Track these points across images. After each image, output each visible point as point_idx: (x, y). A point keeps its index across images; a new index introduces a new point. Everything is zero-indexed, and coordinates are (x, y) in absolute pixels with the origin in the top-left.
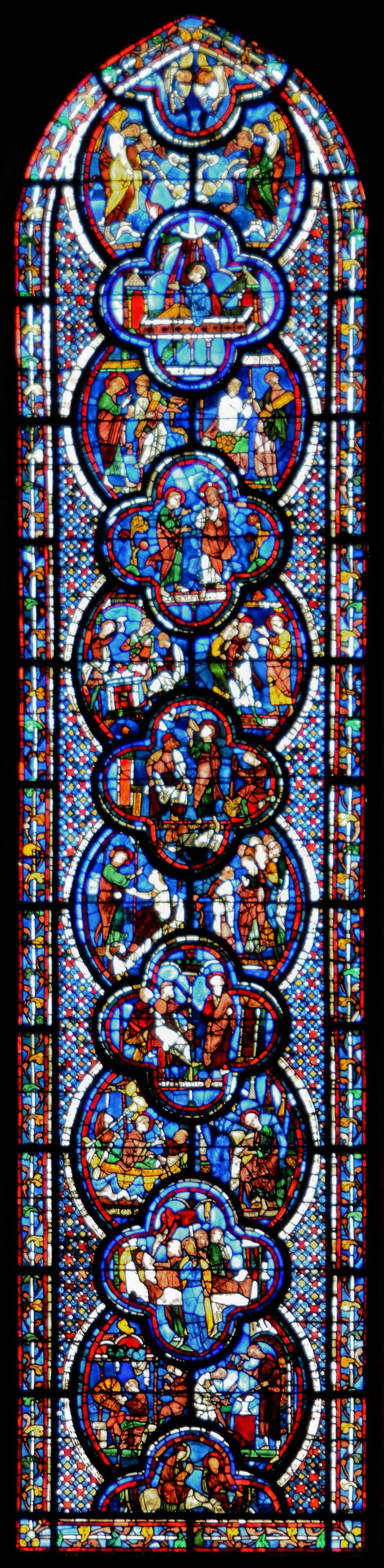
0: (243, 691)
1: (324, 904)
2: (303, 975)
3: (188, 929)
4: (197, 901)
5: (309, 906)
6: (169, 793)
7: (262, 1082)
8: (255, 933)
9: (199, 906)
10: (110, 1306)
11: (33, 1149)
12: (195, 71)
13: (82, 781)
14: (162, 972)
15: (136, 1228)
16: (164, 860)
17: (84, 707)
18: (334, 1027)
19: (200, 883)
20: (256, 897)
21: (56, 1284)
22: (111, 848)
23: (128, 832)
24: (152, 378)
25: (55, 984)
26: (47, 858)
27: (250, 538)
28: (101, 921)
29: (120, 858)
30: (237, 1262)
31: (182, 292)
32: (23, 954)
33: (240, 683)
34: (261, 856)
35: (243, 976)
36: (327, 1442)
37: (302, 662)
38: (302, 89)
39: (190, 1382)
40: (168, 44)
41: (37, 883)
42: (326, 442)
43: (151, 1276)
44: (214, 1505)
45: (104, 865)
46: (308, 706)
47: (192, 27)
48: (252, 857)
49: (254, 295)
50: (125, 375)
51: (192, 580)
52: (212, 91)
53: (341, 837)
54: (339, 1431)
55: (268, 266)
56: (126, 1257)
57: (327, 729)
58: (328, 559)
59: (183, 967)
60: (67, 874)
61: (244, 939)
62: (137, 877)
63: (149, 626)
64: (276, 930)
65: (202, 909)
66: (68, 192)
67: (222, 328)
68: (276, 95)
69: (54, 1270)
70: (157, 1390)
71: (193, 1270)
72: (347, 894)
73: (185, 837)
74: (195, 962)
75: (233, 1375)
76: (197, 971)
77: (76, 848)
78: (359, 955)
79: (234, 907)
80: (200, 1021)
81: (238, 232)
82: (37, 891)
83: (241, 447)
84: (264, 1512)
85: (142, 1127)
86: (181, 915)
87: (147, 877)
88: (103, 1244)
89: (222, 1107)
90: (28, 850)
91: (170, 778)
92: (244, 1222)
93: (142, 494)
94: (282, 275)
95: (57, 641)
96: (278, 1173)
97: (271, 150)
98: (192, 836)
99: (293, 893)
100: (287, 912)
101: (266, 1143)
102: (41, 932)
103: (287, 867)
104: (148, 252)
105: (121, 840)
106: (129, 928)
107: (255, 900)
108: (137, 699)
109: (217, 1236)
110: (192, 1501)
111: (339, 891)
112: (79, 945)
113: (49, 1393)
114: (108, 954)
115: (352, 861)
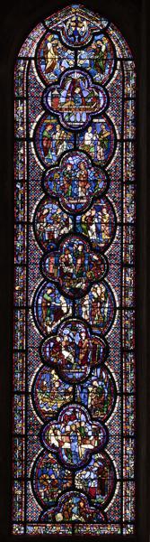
0: (93, 234)
1: (121, 308)
3: (73, 316)
5: (115, 309)
6: (66, 269)
7: (99, 370)
8: (97, 318)
10: (45, 449)
11: (18, 393)
12: (76, 21)
13: (36, 264)
15: (55, 421)
17: (37, 239)
18: (124, 351)
21: (26, 441)
23: (52, 282)
24: (61, 126)
25: (26, 335)
27: (95, 181)
29: (50, 291)
30: (90, 433)
31: (72, 97)
33: (91, 231)
34: (99, 291)
35: (92, 333)
36: (122, 496)
37: (113, 225)
38: (113, 30)
39: (74, 475)
40: (67, 13)
42: (121, 149)
43: (59, 438)
44: (82, 519)
46: (115, 240)
47: (75, 8)
49: (98, 98)
50: (52, 124)
51: (75, 196)
52: (84, 28)
54: (126, 492)
55: (102, 89)
56: (51, 431)
57: (122, 248)
58: (122, 190)
59: (72, 330)
61: (93, 320)
63: (60, 211)
64: (104, 317)
66: (33, 62)
67: (86, 109)
68: (104, 32)
69: (26, 436)
70: (61, 478)
71: (75, 436)
75: (88, 473)
80: (77, 349)
81: (91, 77)
83: (92, 150)
84: (100, 522)
85: (57, 386)
86: (71, 312)
88: (43, 427)
89: (86, 378)
90: (17, 288)
91: (67, 264)
92: (92, 419)
93: (58, 165)
94: (107, 92)
95: (28, 216)
96: (104, 403)
97: (103, 50)
101: (100, 392)
104: (60, 83)
106: (52, 316)
108: (56, 236)
109: (83, 424)
110: (74, 518)
113: (23, 479)
115: (131, 294)
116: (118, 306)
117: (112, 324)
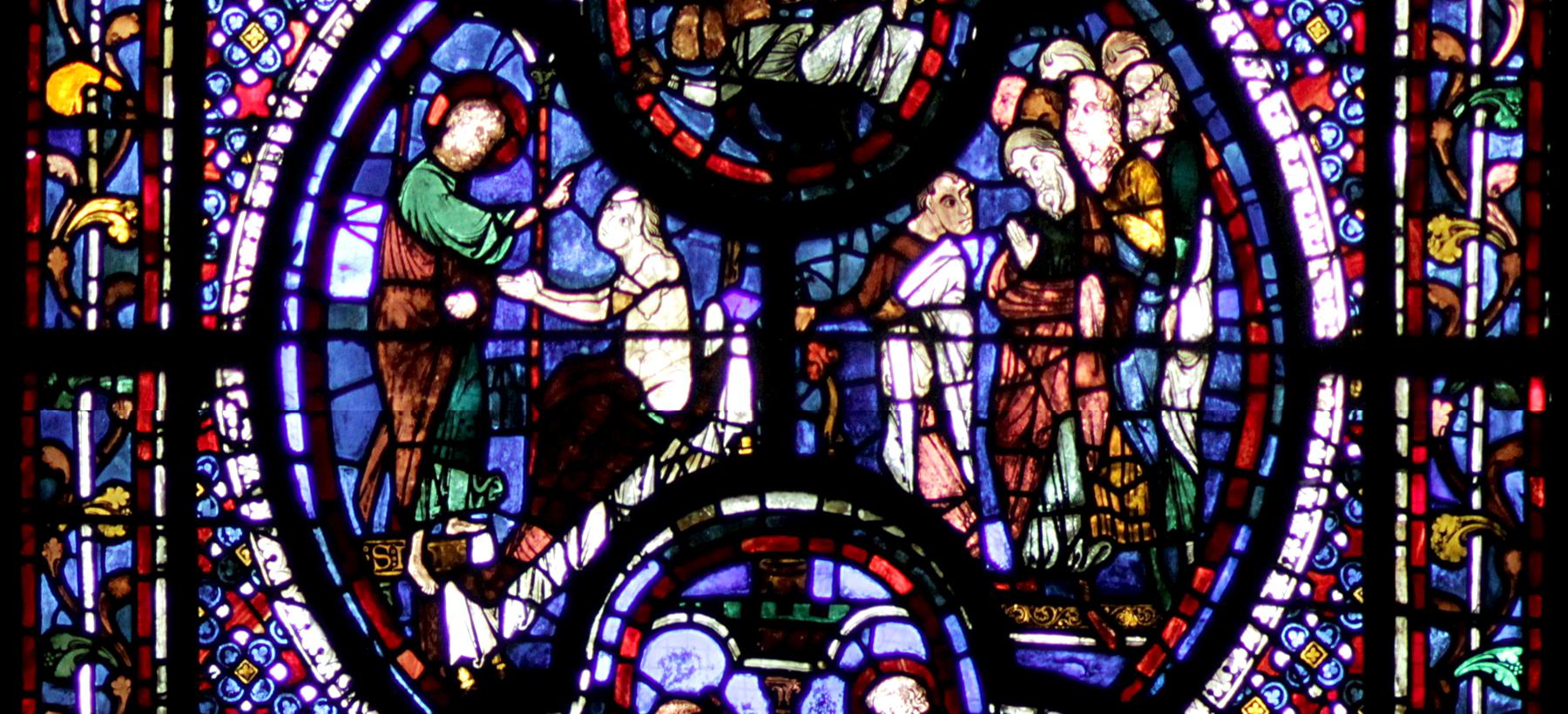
1: (1368, 354)
2: (1276, 675)
4: (812, 332)
5: (1308, 359)
8: (1067, 482)
9: (818, 355)
14: (654, 661)
16: (665, 141)
19: (825, 248)
20: (1074, 318)
22: (430, 83)
26: (151, 124)
28: (386, 417)
32: (42, 566)
34: (1092, 132)
41: (107, 241)
45: (400, 165)
48: (1054, 132)
53: (1446, 47)
59: (748, 637)
60: (238, 205)
61: (1019, 510)
62: (546, 216)
64: (1159, 469)
65: (833, 369)
72: (1471, 314)
73: (759, 37)
74: (800, 613)
76: (813, 652)
77: (279, 83)
78: (1522, 586)
79: (974, 364)
82: (104, 281)
86: (738, 398)
87: (593, 223)
90: (65, 91)
98: (789, 35)
99: (1230, 304)
100: (1206, 390)
102: (121, 465)
103: (1206, 183)
105: (477, 44)
106: (508, 453)
107: (1063, 329)
111: (1439, 297)
112: (290, 527)
114: (416, 569)
115: (1494, 160)
116: (1330, 315)
117: (1264, 557)
